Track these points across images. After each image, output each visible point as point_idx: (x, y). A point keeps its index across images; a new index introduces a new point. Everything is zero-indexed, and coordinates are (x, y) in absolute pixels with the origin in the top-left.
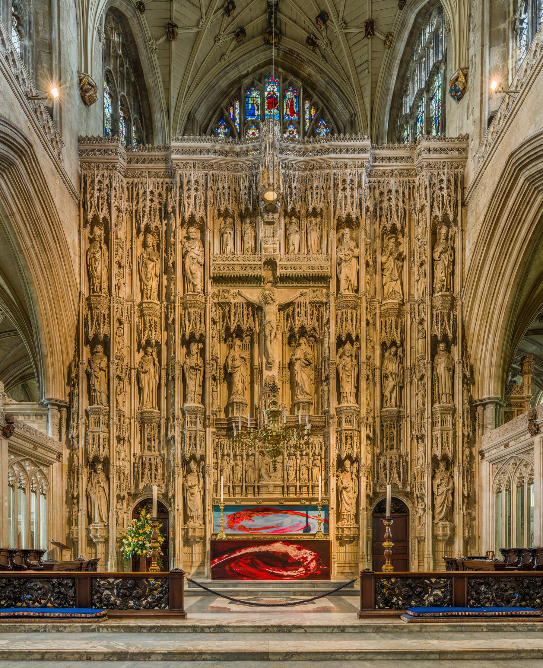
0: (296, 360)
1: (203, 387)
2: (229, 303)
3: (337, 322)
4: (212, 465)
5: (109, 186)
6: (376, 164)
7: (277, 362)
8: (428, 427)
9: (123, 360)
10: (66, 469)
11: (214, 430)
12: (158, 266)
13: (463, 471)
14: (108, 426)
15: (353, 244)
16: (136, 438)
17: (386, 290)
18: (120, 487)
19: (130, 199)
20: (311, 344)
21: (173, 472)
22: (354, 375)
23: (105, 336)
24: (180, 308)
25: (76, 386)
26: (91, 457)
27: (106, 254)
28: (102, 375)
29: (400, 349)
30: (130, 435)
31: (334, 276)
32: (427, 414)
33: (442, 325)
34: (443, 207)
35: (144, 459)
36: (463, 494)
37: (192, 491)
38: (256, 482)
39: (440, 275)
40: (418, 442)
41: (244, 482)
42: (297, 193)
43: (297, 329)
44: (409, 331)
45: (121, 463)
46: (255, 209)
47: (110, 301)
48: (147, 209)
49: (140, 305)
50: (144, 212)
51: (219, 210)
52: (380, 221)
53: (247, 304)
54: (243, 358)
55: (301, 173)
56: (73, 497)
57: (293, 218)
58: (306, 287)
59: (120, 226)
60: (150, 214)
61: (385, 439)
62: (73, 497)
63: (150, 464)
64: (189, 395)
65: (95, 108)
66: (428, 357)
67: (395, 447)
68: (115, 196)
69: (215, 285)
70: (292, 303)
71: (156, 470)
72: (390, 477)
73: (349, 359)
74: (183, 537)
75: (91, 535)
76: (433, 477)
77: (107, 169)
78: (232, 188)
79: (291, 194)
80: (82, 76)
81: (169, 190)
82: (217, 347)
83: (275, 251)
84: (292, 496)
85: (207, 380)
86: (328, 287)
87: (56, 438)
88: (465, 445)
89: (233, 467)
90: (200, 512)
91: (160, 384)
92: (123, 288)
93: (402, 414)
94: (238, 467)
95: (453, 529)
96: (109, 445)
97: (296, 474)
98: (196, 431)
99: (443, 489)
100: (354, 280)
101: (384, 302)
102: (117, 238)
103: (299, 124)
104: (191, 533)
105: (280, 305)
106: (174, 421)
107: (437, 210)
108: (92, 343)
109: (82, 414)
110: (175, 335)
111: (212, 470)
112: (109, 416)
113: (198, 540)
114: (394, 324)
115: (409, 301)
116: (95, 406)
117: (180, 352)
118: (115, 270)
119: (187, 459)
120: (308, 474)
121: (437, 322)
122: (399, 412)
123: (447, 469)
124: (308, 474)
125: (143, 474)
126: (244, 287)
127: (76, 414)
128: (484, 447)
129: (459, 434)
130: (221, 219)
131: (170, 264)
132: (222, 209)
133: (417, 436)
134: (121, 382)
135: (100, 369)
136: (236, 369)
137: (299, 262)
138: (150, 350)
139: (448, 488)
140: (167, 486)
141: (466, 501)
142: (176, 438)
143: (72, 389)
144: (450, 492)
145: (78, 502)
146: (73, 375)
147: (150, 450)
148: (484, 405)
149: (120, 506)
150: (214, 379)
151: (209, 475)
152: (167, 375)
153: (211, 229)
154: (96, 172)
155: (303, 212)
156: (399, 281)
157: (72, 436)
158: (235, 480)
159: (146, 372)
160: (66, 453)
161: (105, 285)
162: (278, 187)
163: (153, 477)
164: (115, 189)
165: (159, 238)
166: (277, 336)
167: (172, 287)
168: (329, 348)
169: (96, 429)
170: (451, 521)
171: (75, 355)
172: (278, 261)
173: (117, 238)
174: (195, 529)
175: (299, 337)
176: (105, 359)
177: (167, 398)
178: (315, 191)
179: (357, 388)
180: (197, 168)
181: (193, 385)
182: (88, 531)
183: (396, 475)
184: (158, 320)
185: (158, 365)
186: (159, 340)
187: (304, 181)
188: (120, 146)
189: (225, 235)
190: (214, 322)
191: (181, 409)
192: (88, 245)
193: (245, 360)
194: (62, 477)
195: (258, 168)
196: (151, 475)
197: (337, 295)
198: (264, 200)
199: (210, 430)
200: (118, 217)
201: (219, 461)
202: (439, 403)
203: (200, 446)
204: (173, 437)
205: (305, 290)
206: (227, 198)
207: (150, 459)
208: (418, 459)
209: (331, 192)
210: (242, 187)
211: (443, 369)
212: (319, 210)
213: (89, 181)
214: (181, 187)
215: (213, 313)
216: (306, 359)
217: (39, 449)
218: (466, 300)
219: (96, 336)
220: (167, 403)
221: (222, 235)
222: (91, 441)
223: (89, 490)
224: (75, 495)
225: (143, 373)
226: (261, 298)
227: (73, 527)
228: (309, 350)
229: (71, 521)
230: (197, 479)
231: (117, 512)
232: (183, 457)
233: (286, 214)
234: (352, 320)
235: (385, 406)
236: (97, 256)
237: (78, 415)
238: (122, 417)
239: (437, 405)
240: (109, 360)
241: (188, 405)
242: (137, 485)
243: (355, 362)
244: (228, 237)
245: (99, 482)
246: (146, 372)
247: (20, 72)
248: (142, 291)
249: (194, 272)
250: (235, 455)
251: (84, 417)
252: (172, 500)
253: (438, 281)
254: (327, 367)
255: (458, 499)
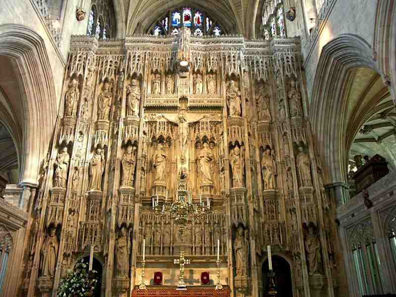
0: (201, 157)
1: (135, 175)
2: (156, 122)
3: (228, 133)
4: (138, 231)
5: (86, 59)
6: (248, 48)
7: (187, 158)
8: (297, 203)
9: (80, 157)
10: (28, 232)
11: (141, 205)
12: (110, 101)
13: (326, 234)
14: (64, 202)
15: (236, 89)
16: (83, 210)
17: (260, 115)
18: (67, 246)
19: (98, 65)
20: (211, 147)
21: (108, 236)
22: (242, 167)
23: (70, 142)
24: (123, 124)
25: (46, 174)
26: (48, 224)
27: (78, 94)
28: (65, 167)
29: (273, 151)
30: (79, 208)
31: (225, 106)
32: (296, 193)
33: (299, 135)
34: (290, 71)
35: (87, 226)
36: (328, 252)
37: (122, 251)
38: (171, 244)
39: (294, 107)
40: (291, 214)
41: (162, 244)
42: (200, 62)
43: (201, 138)
44: (277, 139)
45: (70, 229)
46: (174, 70)
47: (76, 121)
48: (107, 70)
49: (97, 122)
50: (105, 71)
51: (152, 70)
52: (253, 77)
53: (167, 122)
54: (163, 156)
55: (203, 52)
56: (30, 255)
57: (198, 75)
58: (207, 113)
59: (89, 79)
60: (109, 72)
61: (267, 212)
62: (30, 255)
63: (92, 230)
64: (124, 180)
65: (84, 22)
66: (292, 156)
67: (275, 218)
68: (89, 63)
69: (146, 111)
70: (198, 122)
71: (96, 234)
72: (273, 240)
73: (238, 157)
74: (112, 288)
75: (39, 286)
76: (305, 239)
77: (85, 50)
78: (161, 59)
79: (197, 62)
80: (78, 8)
81: (122, 60)
82: (145, 149)
83: (187, 92)
84: (198, 255)
85: (137, 171)
86: (222, 113)
87: (25, 210)
88: (325, 216)
89: (154, 233)
90: (127, 268)
91: (104, 173)
92: (86, 113)
93: (278, 194)
94: (157, 233)
95: (325, 279)
96: (63, 216)
97: (202, 238)
98: (127, 205)
99: (312, 249)
100: (238, 109)
101: (259, 122)
102: (86, 85)
103: (203, 28)
104: (118, 285)
105: (189, 123)
106: (112, 198)
107: (287, 72)
108: (60, 148)
109: (46, 193)
110: (117, 141)
111: (138, 235)
112: (66, 195)
113: (125, 290)
114: (267, 135)
115: (275, 121)
116: (56, 188)
117: (119, 153)
118: (82, 103)
119: (120, 226)
120: (211, 238)
121: (295, 134)
122: (276, 192)
123: (314, 233)
124: (211, 238)
125: (85, 237)
126: (166, 113)
127: (42, 193)
128: (339, 217)
129: (320, 207)
130: (153, 75)
131: (118, 99)
132: (154, 70)
133: (290, 209)
134: (77, 172)
135: (64, 163)
136: (159, 164)
137: (202, 99)
138: (99, 150)
139: (317, 247)
140: (102, 247)
141: (331, 257)
142: (112, 211)
143: (43, 176)
144: (319, 250)
145: (33, 259)
146: (45, 167)
147: (93, 219)
148: (334, 188)
149: (64, 262)
150: (143, 169)
151: (135, 238)
152: (110, 167)
153: (147, 79)
154: (79, 52)
155: (205, 71)
156: (267, 110)
157: (37, 210)
158: (155, 243)
159: (96, 165)
160: (30, 221)
161: (75, 111)
162: (189, 59)
163: (93, 239)
164: (89, 60)
165: (113, 85)
166: (188, 142)
167: (118, 112)
168: (224, 149)
169: (55, 204)
170: (324, 273)
171: (48, 154)
172: (188, 98)
173: (86, 85)
174: (122, 281)
175: (203, 143)
176: (68, 157)
177: (108, 182)
178: (212, 61)
179: (244, 176)
180: (140, 49)
181: (128, 173)
182: (37, 282)
183: (277, 238)
184: (107, 132)
185: (104, 160)
186: (107, 145)
187: (205, 56)
188: (95, 40)
189: (155, 84)
190: (144, 133)
191: (118, 190)
192: (67, 89)
193: (165, 157)
194: (24, 238)
195: (177, 50)
196: (91, 238)
197: (228, 117)
198: (179, 65)
199: (137, 205)
200: (89, 74)
201: (143, 228)
202: (303, 186)
203: (130, 216)
204: (110, 210)
205: (206, 114)
206: (157, 64)
207: (92, 226)
208: (293, 226)
209: (222, 61)
210: (167, 59)
211: (302, 165)
212: (214, 71)
213: (73, 57)
214: (129, 59)
215: (144, 128)
216: (208, 157)
217: (11, 218)
218: (312, 121)
219: (64, 142)
220: (108, 186)
221: (153, 83)
222: (50, 212)
223: (43, 249)
224: (32, 253)
225: (94, 165)
226: (177, 119)
227: (25, 279)
228: (210, 151)
229: (26, 274)
230: (126, 242)
231: (62, 267)
232: (117, 224)
233: (194, 72)
234: (238, 132)
235: (265, 188)
236: (73, 95)
237: (43, 194)
238: (75, 196)
239: (301, 188)
240: (70, 157)
241: (123, 187)
242: (80, 246)
243: (242, 159)
244: (157, 85)
245: (51, 243)
246: (96, 165)
247: (43, 8)
248: (98, 114)
249: (133, 104)
250: (156, 223)
251: (48, 195)
252: (106, 258)
253: (293, 110)
254: (222, 162)
255: (326, 256)
